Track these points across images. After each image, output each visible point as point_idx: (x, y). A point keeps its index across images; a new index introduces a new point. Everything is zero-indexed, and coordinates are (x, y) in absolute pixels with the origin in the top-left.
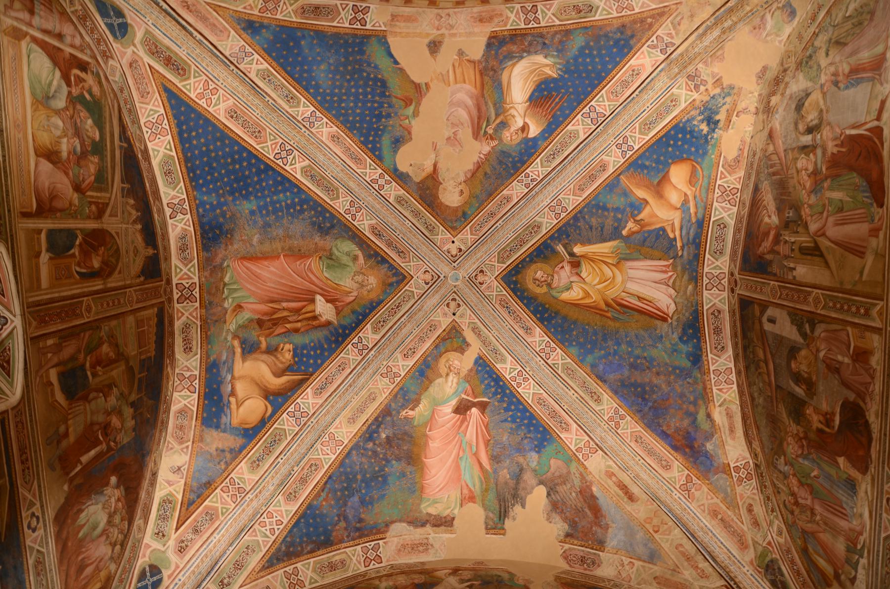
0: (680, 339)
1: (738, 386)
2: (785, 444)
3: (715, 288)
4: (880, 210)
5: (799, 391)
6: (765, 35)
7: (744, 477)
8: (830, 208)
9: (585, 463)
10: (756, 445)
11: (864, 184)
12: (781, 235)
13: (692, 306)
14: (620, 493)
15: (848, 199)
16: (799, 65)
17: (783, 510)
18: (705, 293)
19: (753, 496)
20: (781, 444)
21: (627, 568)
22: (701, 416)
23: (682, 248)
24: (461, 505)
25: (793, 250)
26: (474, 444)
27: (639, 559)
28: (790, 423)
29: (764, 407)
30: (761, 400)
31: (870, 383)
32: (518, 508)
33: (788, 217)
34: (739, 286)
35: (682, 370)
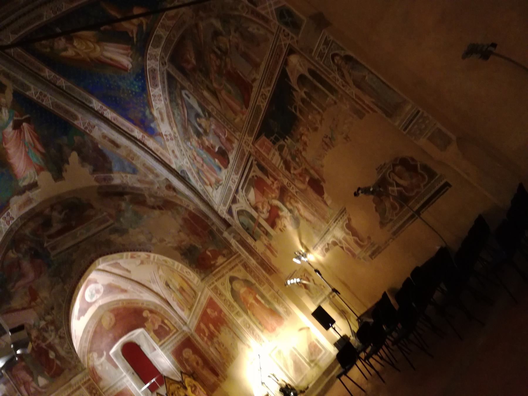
1: (165, 102)
2: (191, 140)
5: (201, 130)
9: (91, 134)
10: (175, 129)
14: (112, 145)
17: (189, 157)
18: (148, 62)
21: (125, 178)
22: (147, 112)
23: (137, 42)
24: (38, 174)
26: (32, 142)
27: (129, 173)
32: (66, 166)
35: (136, 93)
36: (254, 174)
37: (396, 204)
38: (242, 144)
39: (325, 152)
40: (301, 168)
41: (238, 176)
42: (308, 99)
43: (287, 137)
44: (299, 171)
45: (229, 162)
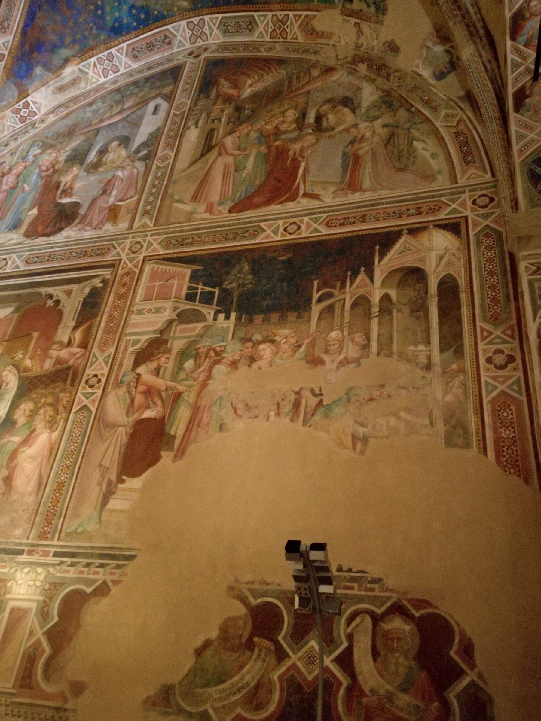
0: (133, 6)
1: (103, 84)
2: (50, 151)
3: (191, 32)
4: (226, 211)
5: (92, 156)
6: (429, 44)
7: (22, 114)
8: (241, 156)
10: (52, 118)
11: (252, 191)
12: (230, 104)
13: (167, 11)
15: (244, 175)
16: (387, 93)
18: (184, 23)
19: (6, 128)
20: (51, 146)
25: (213, 121)
28: (67, 151)
29: (82, 118)
30: (89, 114)
31: (91, 226)
33: (245, 108)
34: (193, 61)
35: (102, 17)
36: (62, 297)
37: (276, 696)
38: (127, 238)
39: (272, 413)
40: (172, 384)
41: (23, 267)
42: (375, 310)
43: (233, 315)
44: (159, 383)
45: (48, 235)
